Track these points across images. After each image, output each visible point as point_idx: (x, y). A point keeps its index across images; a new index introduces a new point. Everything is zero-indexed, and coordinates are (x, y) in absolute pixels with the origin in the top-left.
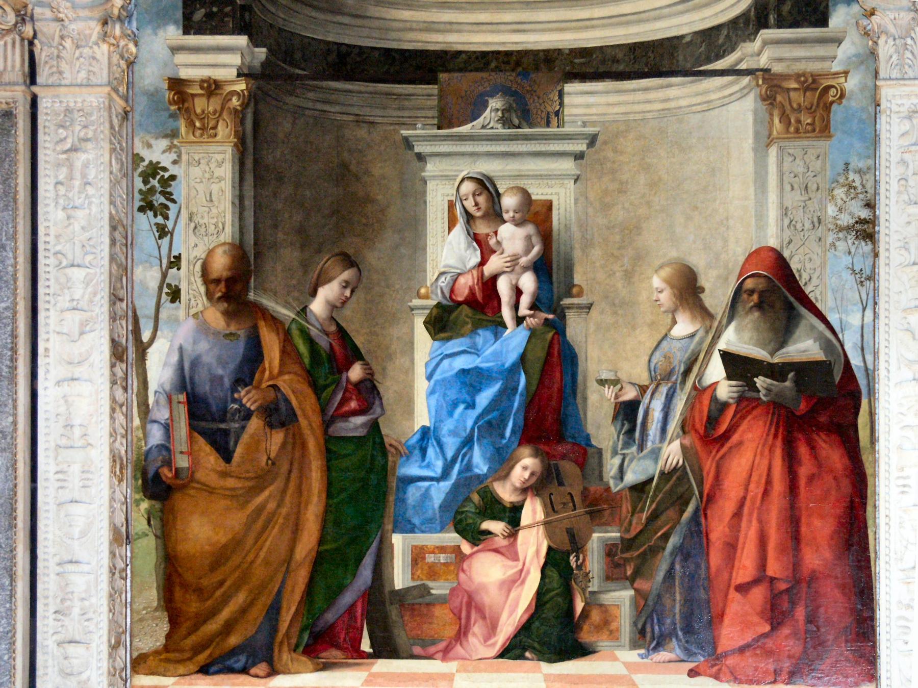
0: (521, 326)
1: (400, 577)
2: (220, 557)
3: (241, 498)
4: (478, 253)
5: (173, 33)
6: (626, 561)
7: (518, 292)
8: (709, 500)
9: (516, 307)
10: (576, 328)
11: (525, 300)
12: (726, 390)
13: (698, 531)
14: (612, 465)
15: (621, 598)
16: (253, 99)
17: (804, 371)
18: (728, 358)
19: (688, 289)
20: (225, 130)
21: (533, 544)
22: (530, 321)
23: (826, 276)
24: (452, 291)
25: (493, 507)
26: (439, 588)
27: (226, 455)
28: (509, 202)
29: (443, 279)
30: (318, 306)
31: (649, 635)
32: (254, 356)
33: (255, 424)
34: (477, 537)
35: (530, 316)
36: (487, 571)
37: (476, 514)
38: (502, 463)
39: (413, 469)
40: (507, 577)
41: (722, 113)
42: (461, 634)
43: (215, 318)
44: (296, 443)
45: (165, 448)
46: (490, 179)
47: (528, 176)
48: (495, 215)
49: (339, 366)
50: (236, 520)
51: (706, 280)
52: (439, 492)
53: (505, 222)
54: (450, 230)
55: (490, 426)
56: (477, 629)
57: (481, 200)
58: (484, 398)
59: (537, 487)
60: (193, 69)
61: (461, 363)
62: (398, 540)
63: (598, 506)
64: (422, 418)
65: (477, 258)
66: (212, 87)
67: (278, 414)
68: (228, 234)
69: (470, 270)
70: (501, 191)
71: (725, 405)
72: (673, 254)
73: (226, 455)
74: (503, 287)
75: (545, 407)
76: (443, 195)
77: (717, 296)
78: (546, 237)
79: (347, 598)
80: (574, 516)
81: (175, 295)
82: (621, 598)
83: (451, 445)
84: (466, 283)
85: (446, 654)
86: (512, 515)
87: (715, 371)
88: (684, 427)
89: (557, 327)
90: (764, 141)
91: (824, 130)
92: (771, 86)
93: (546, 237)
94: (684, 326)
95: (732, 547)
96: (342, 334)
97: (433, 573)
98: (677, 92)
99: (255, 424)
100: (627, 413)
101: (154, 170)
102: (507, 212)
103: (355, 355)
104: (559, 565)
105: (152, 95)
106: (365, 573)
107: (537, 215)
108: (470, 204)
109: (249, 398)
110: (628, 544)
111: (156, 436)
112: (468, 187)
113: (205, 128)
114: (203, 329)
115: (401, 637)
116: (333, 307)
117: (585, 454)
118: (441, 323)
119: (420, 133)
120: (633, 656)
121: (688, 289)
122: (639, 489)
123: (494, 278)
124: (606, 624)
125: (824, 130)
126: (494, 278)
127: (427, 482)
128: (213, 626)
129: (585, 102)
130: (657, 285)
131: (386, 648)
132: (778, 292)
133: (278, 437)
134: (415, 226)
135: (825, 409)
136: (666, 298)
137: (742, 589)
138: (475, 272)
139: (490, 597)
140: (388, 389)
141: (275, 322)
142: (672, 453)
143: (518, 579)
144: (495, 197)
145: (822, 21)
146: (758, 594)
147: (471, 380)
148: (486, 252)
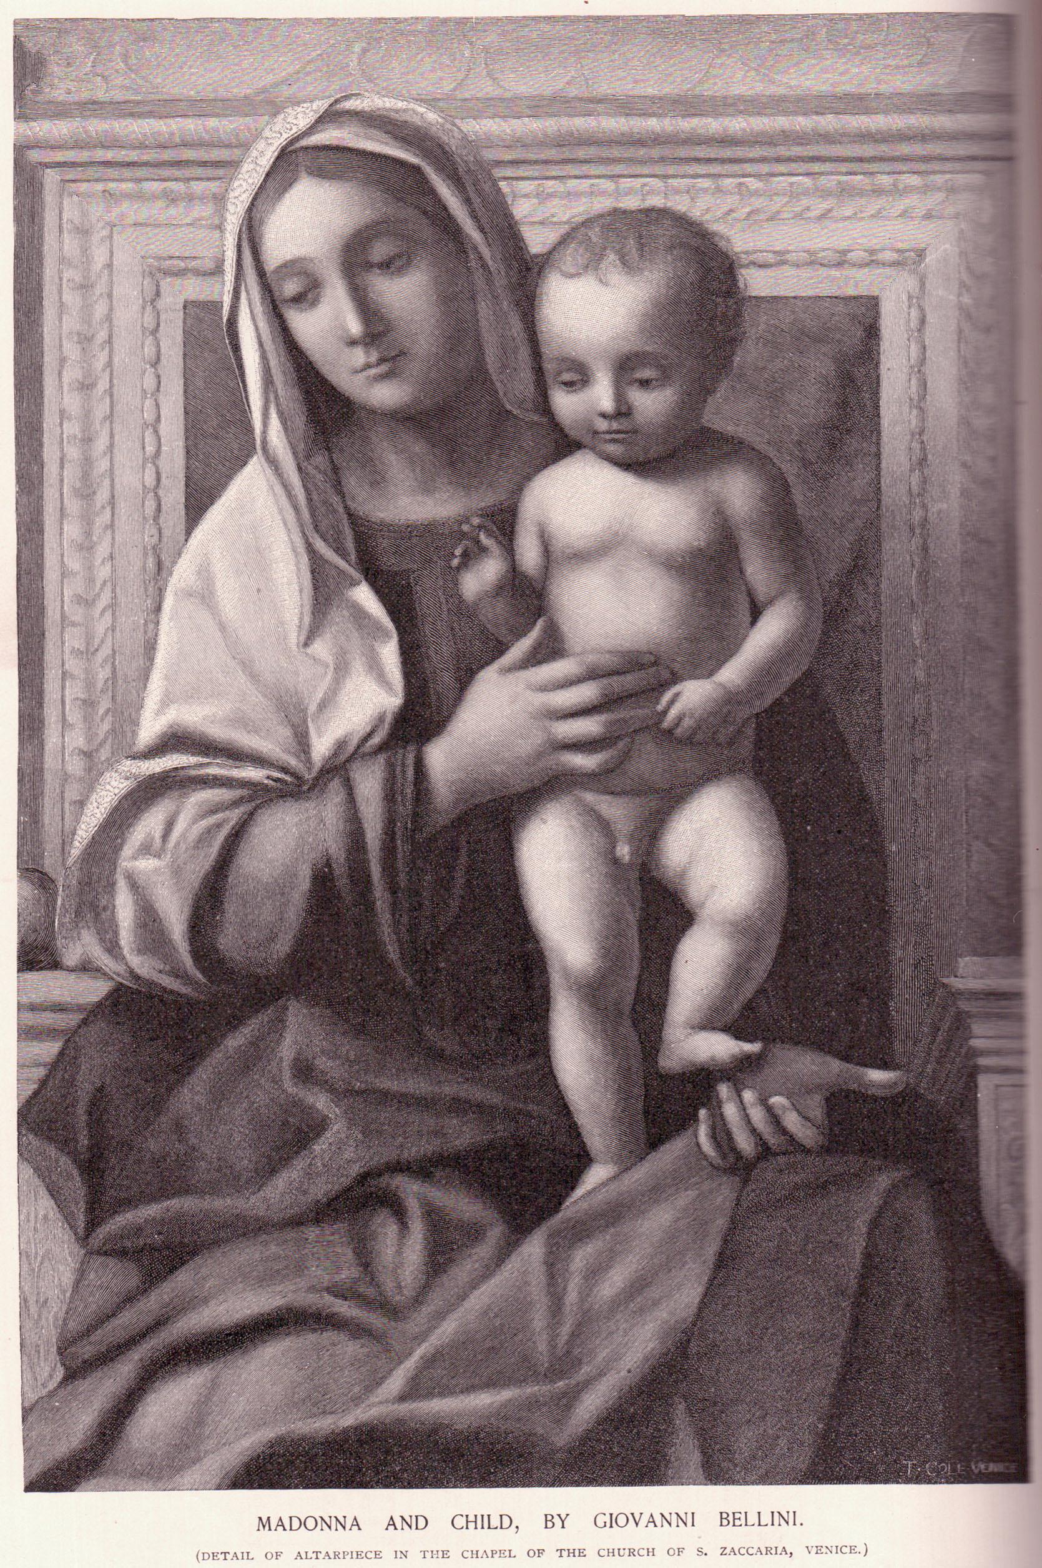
0: (673, 1150)
4: (390, 653)
7: (654, 911)
9: (635, 1002)
11: (700, 965)
22: (740, 1111)
24: (210, 897)
28: (592, 310)
29: (151, 823)
35: (739, 1071)
46: (473, 177)
47: (725, 154)
48: (493, 413)
53: (563, 444)
54: (198, 501)
57: (407, 294)
65: (368, 698)
69: (339, 767)
70: (537, 241)
74: (556, 872)
76: (161, 271)
102: (579, 376)
108: (326, 323)
112: (310, 221)
123: (496, 816)
126: (496, 816)
138: (369, 783)
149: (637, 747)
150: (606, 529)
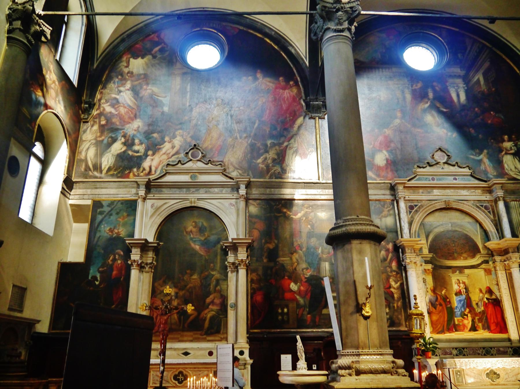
1: (456, 323)
2: (437, 321)
3: (438, 314)
6: (480, 320)
8: (487, 314)
10: (470, 295)
12: (487, 302)
13: (487, 317)
14: (476, 310)
15: (480, 324)
16: (433, 271)
17: (494, 299)
18: (486, 298)
19: (481, 291)
20: (431, 274)
21: (470, 319)
23: (495, 289)
26: (461, 324)
27: (436, 309)
28: (461, 282)
30: (443, 293)
31: (484, 329)
32: (437, 298)
33: (438, 306)
34: (464, 318)
36: (466, 322)
37: (463, 315)
38: (465, 310)
40: (468, 322)
41: (480, 273)
42: (464, 329)
43: (432, 294)
44: (443, 308)
48: (460, 283)
49: (446, 300)
50: (438, 316)
51: (483, 290)
52: (459, 313)
55: (463, 306)
56: (466, 328)
58: (462, 302)
59: (469, 312)
61: (459, 299)
62: (455, 318)
63: (476, 314)
64: (456, 305)
66: (429, 270)
67: (441, 305)
68: (432, 285)
71: (486, 303)
72: (478, 287)
73: (436, 309)
75: (468, 303)
77: (484, 291)
78: (465, 285)
79: (451, 325)
80: (473, 315)
82: (480, 324)
83: (459, 308)
84: (458, 290)
85: (463, 331)
86: (467, 315)
87: (485, 300)
88: (483, 306)
89: (468, 295)
90: (485, 275)
91: (491, 274)
92: (485, 270)
93: (465, 285)
94: (481, 295)
95: (491, 319)
96: (446, 296)
97: (460, 322)
99: (438, 306)
100: (477, 304)
103: (448, 298)
104: (473, 321)
107: (464, 283)
109: (437, 303)
113: (428, 274)
114: (431, 295)
115: (458, 329)
116: (445, 293)
117: (474, 309)
118: (456, 294)
119: (451, 274)
120: (483, 331)
121: (481, 291)
122: (480, 312)
124: (479, 328)
125: (491, 274)
127: (458, 312)
129: (467, 271)
130: (478, 290)
131: (456, 331)
132: (490, 291)
133: (441, 308)
134: (452, 284)
135: (497, 303)
136: (479, 292)
139: (466, 325)
140: (452, 302)
141: (439, 295)
142: (482, 308)
143: (469, 323)
144: (459, 281)
145: (488, 263)
146: (494, 324)
147: (460, 301)
150: (462, 285)
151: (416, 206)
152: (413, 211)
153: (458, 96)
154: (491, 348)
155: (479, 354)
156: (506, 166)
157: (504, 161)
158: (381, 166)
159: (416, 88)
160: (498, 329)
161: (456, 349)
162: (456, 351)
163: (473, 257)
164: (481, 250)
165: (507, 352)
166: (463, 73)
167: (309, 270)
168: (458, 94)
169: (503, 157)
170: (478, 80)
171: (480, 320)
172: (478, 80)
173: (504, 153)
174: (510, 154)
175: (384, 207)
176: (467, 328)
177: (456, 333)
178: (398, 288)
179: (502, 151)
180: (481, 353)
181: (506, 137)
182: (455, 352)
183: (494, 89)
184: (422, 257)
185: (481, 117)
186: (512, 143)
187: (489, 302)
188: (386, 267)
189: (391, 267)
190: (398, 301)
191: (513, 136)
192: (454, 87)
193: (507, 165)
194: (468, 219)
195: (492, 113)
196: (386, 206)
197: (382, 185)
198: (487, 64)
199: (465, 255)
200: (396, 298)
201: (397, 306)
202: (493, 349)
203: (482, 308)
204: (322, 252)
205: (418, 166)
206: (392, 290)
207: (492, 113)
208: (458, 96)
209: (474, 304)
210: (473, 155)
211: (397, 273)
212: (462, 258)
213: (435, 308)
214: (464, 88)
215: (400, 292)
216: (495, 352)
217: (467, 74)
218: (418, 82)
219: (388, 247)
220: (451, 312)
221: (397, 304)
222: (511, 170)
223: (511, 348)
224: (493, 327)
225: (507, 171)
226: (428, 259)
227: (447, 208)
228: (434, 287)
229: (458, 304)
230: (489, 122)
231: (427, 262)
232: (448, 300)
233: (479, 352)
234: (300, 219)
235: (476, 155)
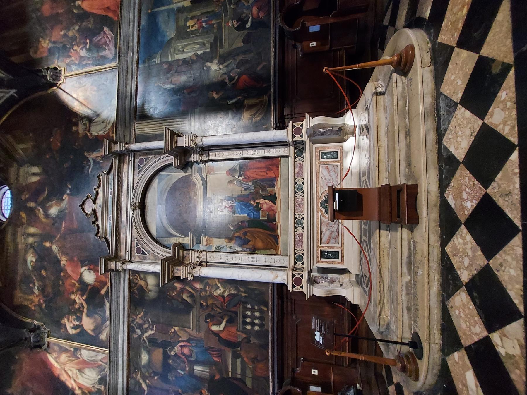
2: (263, 242)
3: (256, 239)
5: (200, 245)
8: (256, 179)
14: (252, 191)
19: (230, 182)
20: (211, 239)
21: (261, 201)
25: (257, 206)
30: (232, 228)
31: (273, 186)
33: (246, 237)
34: (261, 208)
36: (265, 207)
37: (258, 208)
38: (251, 205)
39: (252, 216)
40: (266, 204)
42: (273, 210)
43: (233, 241)
44: (248, 232)
45: (249, 249)
56: (272, 208)
58: (243, 207)
60: (204, 244)
61: (239, 210)
63: (257, 193)
64: (246, 215)
66: (207, 240)
71: (245, 178)
77: (232, 178)
81: (231, 246)
84: (229, 209)
85: (276, 212)
86: (258, 204)
87: (240, 178)
95: (262, 176)
98: (208, 184)
101: (216, 248)
104: (264, 198)
105: (208, 248)
106: (265, 223)
110: (261, 189)
111: (248, 250)
113: (211, 242)
114: (235, 243)
120: (276, 188)
121: (230, 182)
124: (271, 191)
127: (253, 214)
128: (272, 243)
131: (275, 220)
133: (248, 234)
137: (267, 174)
139: (268, 206)
141: (234, 234)
142: (250, 183)
143: (266, 202)
148: (226, 207)
149: (228, 204)
151: (137, 245)
152: (142, 249)
153: (35, 174)
154: (295, 183)
155: (302, 200)
156: (100, 133)
157: (96, 134)
158: (95, 277)
159: (25, 219)
160: (274, 168)
161: (295, 228)
162: (298, 228)
163: (194, 185)
164: (187, 174)
165: (300, 163)
166: (15, 165)
167: (203, 392)
168: (32, 175)
169: (92, 135)
170: (22, 149)
171: (264, 189)
172: (22, 149)
173: (88, 133)
174: (89, 127)
175: (137, 283)
176: (273, 206)
177: (277, 221)
178: (224, 288)
179: (87, 135)
180: (301, 197)
181: (74, 128)
182: (299, 230)
183: (31, 134)
184: (193, 246)
185: (55, 153)
186: (79, 123)
187: (244, 175)
188: (200, 296)
189: (201, 291)
190: (239, 291)
191: (74, 120)
192: (27, 178)
193: (100, 131)
194: (155, 183)
195: (51, 140)
196: (136, 281)
197: (113, 281)
198: (10, 138)
199: (192, 194)
200: (235, 292)
201: (244, 292)
202: (296, 181)
203: (250, 183)
204: (183, 370)
205: (97, 235)
206: (226, 294)
207: (51, 140)
208: (35, 174)
209: (244, 193)
210: (89, 168)
211: (208, 284)
212: (195, 198)
213: (249, 241)
214: (28, 167)
215: (229, 285)
216: (301, 179)
217: (16, 161)
218: (21, 216)
219: (178, 289)
220: (254, 223)
221: (242, 292)
222: (104, 128)
223: (295, 158)
224: (271, 174)
225: (106, 133)
226: (195, 239)
227: (142, 207)
228: (226, 238)
229: (245, 213)
230: (59, 144)
231: (199, 242)
232: (240, 224)
233: (299, 199)
234: (148, 386)
235: (89, 165)
